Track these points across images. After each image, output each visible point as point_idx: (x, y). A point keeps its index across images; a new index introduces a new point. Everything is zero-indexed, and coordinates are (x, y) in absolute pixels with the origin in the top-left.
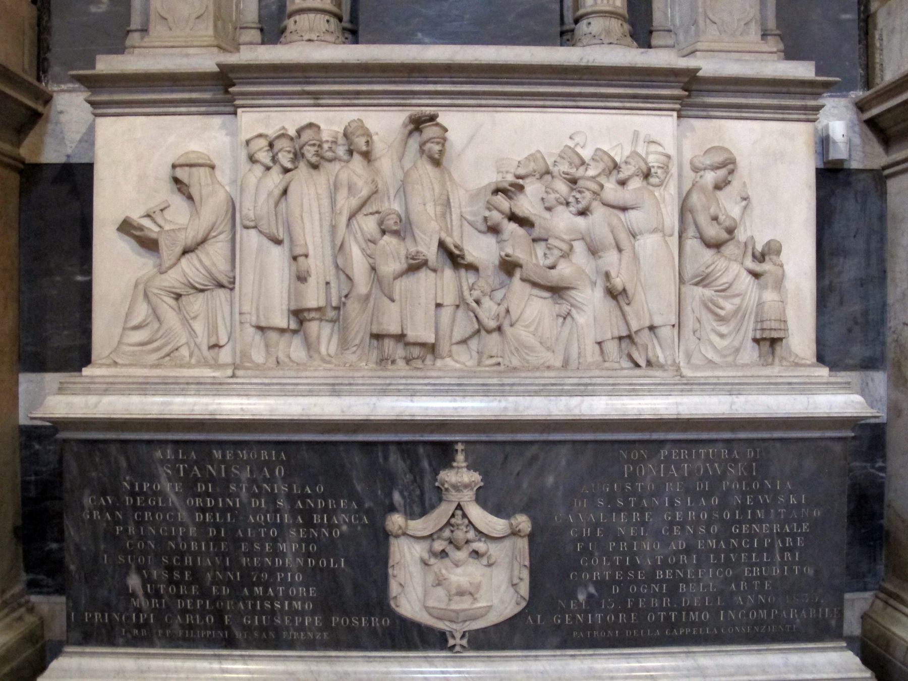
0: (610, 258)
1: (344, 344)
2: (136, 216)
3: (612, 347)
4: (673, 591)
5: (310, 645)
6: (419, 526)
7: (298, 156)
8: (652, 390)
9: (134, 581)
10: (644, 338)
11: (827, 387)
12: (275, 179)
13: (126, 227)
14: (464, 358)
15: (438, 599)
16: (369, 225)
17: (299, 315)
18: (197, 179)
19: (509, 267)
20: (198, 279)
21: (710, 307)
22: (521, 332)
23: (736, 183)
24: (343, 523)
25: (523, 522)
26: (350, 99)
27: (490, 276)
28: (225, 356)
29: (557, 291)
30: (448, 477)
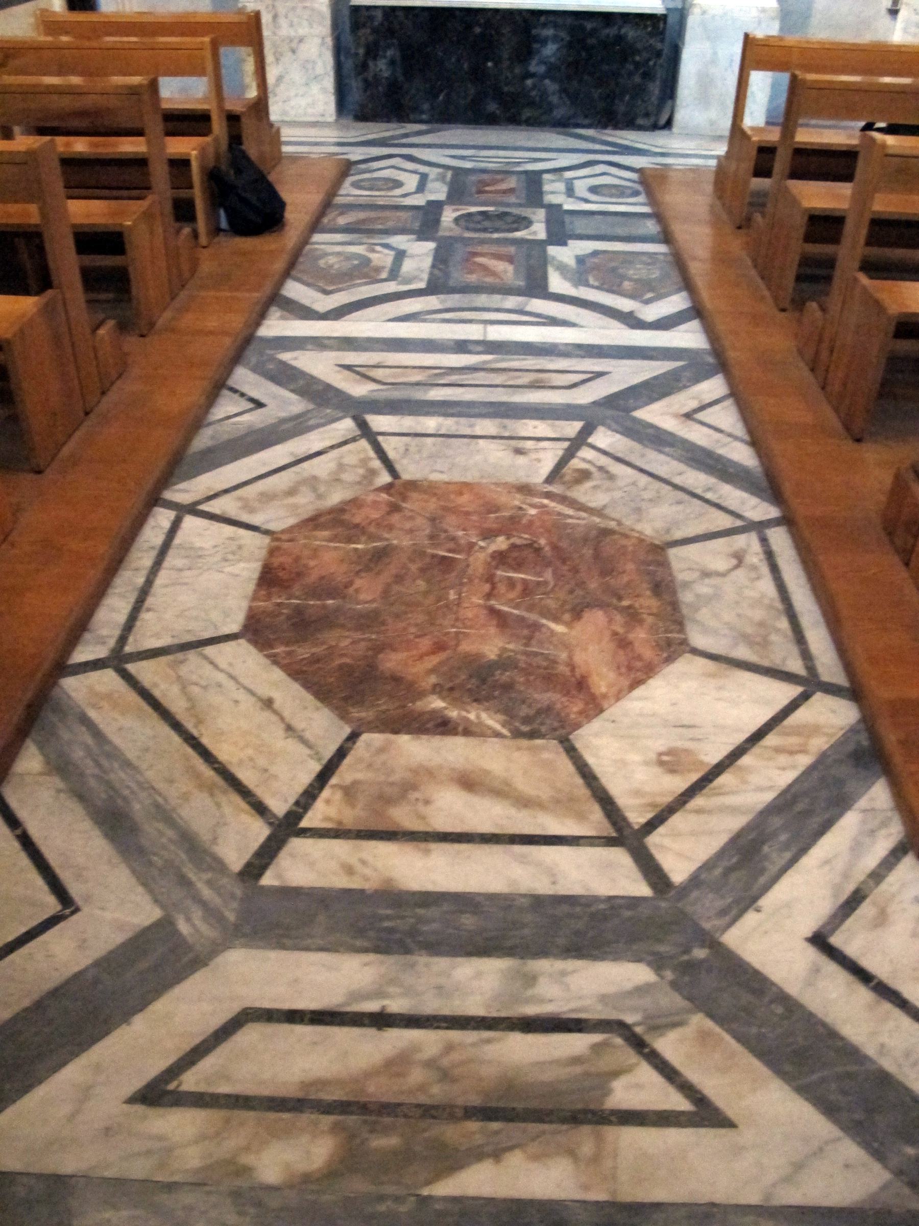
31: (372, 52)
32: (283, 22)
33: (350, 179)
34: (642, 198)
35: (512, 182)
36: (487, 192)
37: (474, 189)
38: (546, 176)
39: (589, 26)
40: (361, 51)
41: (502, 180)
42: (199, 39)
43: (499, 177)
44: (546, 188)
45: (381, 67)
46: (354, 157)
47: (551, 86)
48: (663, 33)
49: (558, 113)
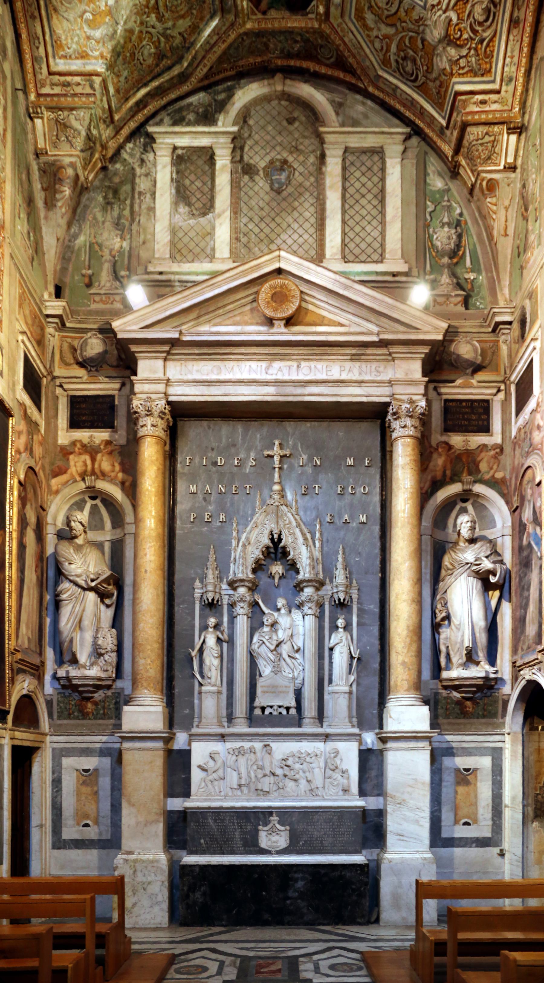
0: (307, 774)
1: (249, 791)
2: (201, 763)
3: (308, 792)
4: (322, 843)
5: (241, 854)
6: (265, 828)
7: (239, 752)
8: (316, 800)
9: (202, 841)
10: (315, 790)
11: (357, 800)
12: (234, 758)
13: (199, 767)
14: (276, 794)
15: (269, 843)
16: (255, 767)
17: (240, 786)
18: (216, 757)
19: (285, 776)
20: (216, 778)
21: (331, 784)
22: (288, 789)
23: (339, 757)
24: (249, 828)
25: (288, 828)
26: (251, 740)
27: (281, 777)
28: (222, 794)
29: (296, 780)
30: (271, 818)
31: (192, 888)
32: (139, 874)
33: (175, 967)
34: (364, 972)
35: (279, 965)
36: (263, 973)
37: (254, 972)
38: (301, 959)
39: (323, 872)
40: (185, 888)
41: (272, 964)
42: (82, 897)
43: (271, 961)
44: (301, 967)
45: (198, 896)
46: (177, 952)
47: (301, 904)
48: (368, 873)
49: (306, 918)
